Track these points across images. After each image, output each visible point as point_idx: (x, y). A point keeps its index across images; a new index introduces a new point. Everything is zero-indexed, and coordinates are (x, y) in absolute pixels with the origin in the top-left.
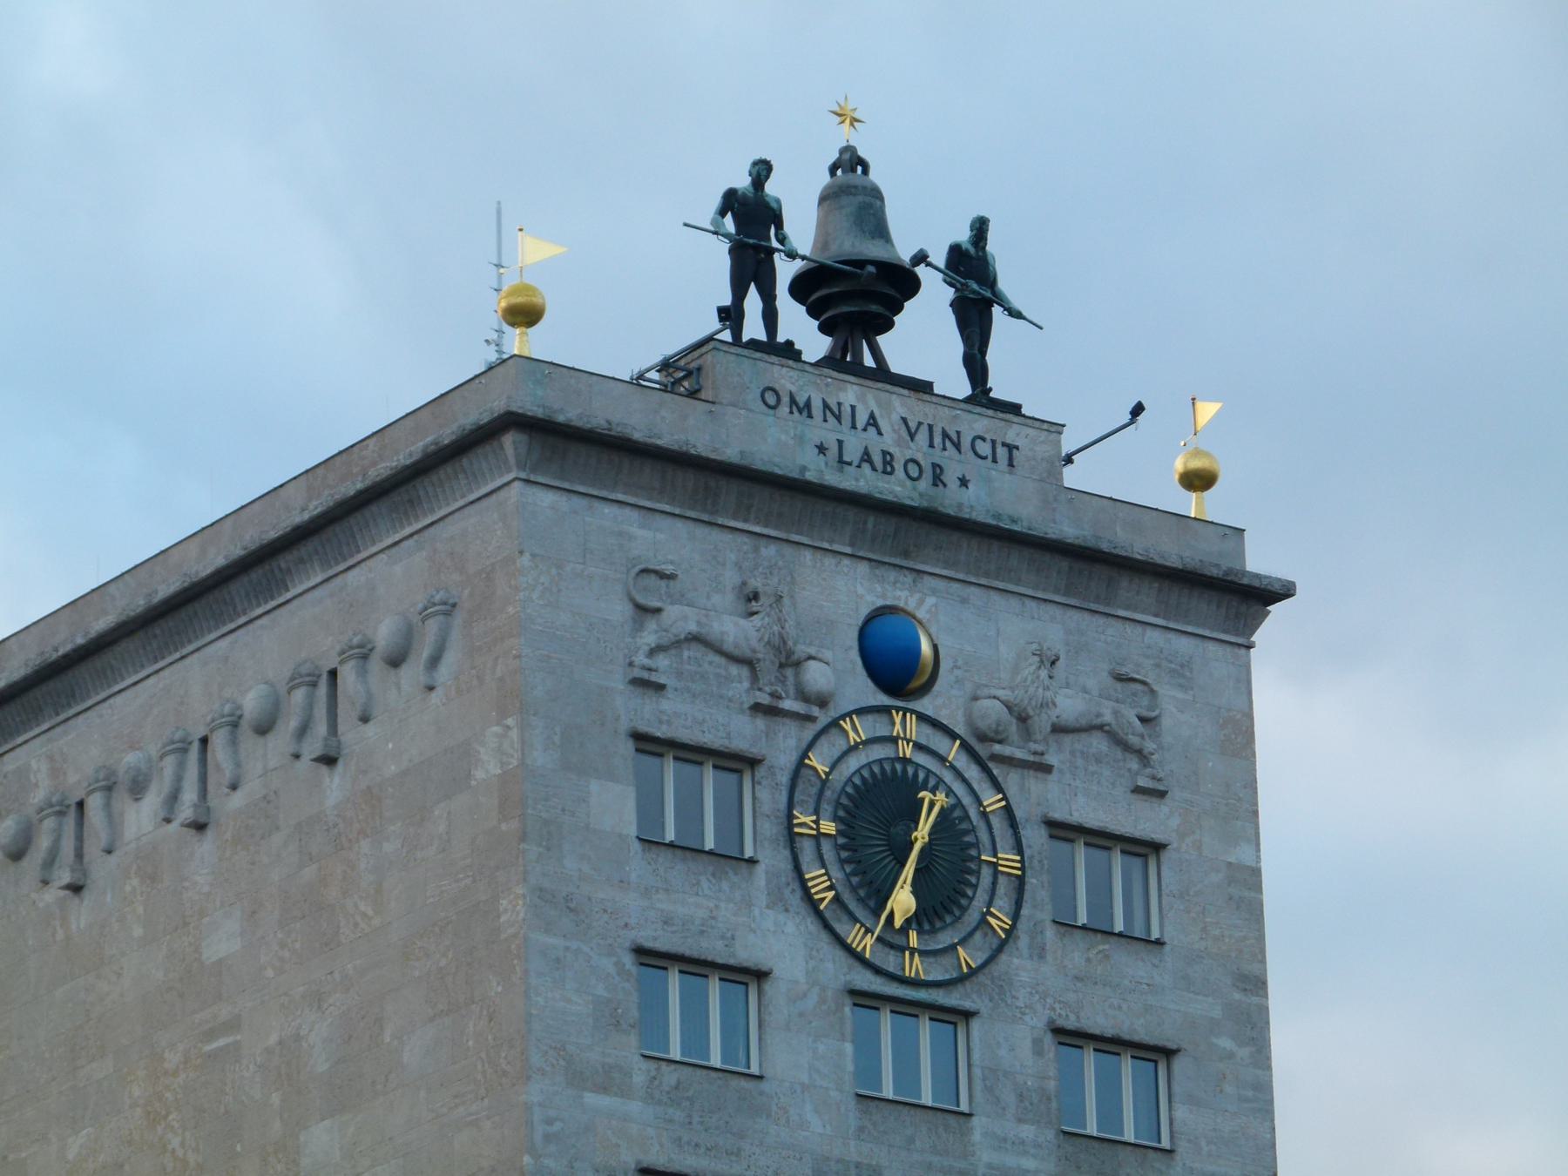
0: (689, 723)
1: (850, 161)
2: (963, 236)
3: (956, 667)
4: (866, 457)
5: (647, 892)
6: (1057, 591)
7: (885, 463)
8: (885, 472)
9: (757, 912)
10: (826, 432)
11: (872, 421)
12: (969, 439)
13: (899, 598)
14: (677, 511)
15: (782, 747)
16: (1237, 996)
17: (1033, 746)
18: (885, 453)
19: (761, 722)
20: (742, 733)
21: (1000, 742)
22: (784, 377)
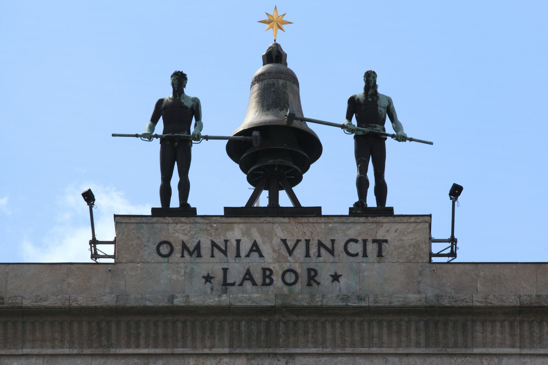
1: (275, 56)
2: (359, 91)
7: (265, 277)
8: (264, 284)
11: (255, 248)
12: (343, 243)
18: (264, 270)
22: (178, 232)
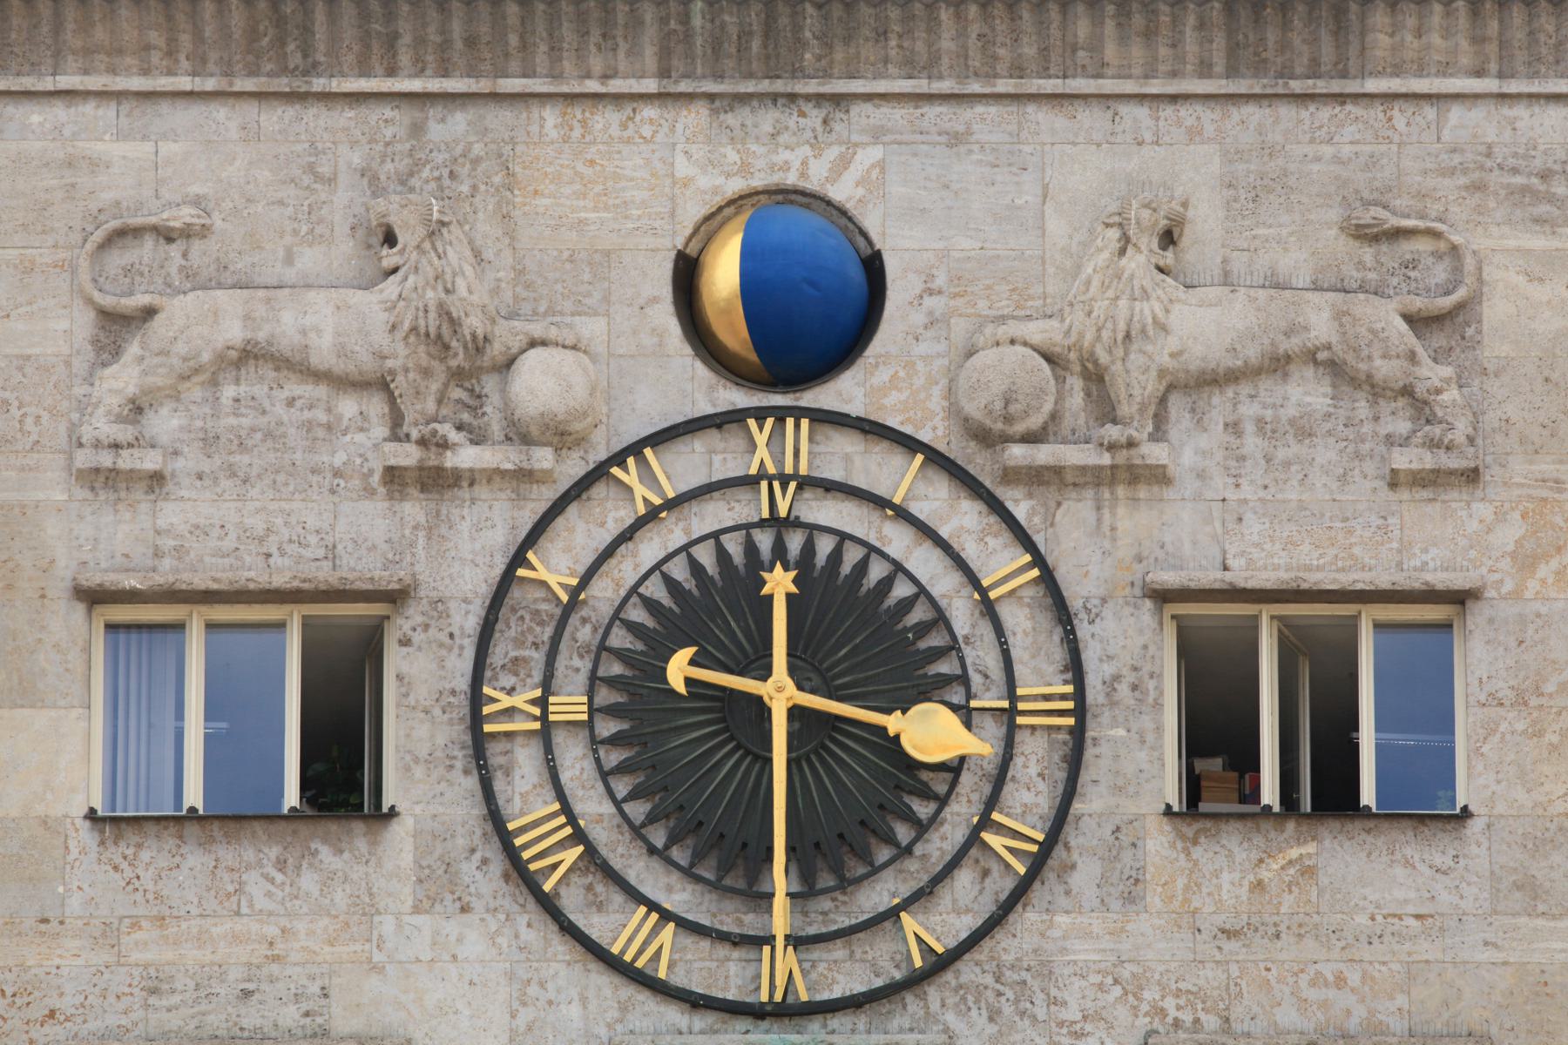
0: (229, 543)
3: (931, 292)
5: (108, 934)
9: (387, 925)
13: (786, 167)
17: (1113, 432)
19: (414, 509)
21: (1031, 438)
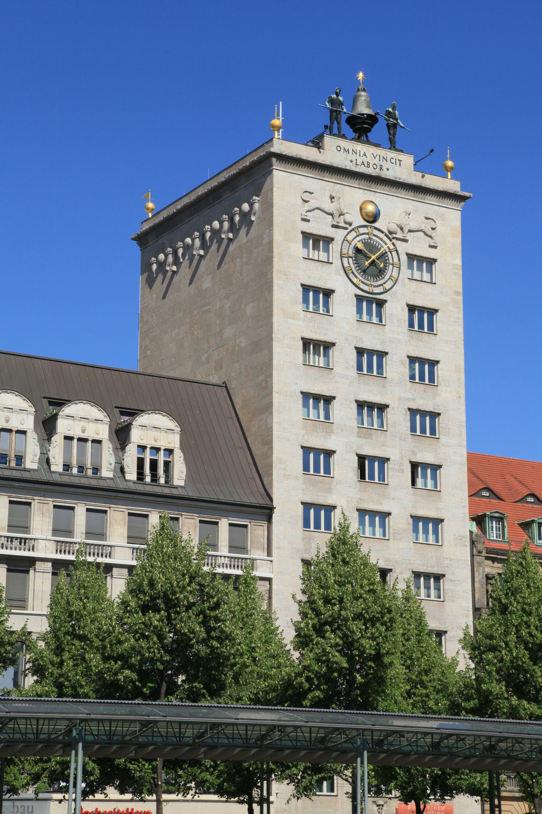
4: (363, 163)
6: (411, 197)
7: (368, 165)
10: (353, 157)
11: (365, 154)
14: (314, 177)
15: (339, 235)
16: (455, 296)
19: (334, 229)
20: (329, 232)
